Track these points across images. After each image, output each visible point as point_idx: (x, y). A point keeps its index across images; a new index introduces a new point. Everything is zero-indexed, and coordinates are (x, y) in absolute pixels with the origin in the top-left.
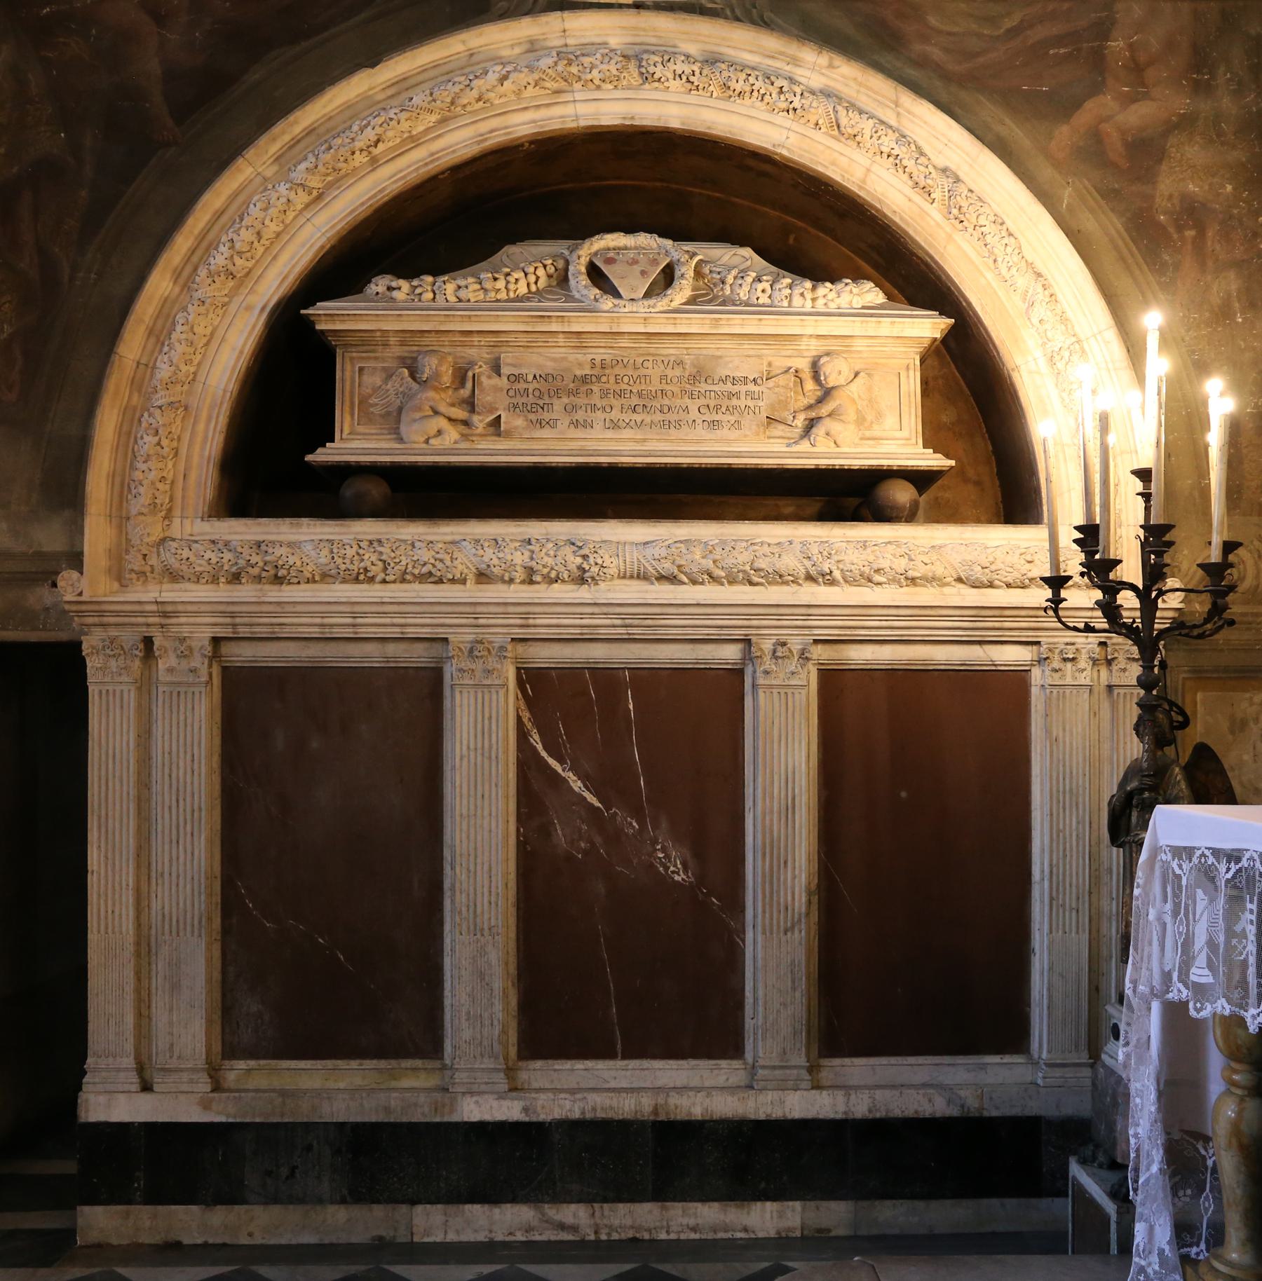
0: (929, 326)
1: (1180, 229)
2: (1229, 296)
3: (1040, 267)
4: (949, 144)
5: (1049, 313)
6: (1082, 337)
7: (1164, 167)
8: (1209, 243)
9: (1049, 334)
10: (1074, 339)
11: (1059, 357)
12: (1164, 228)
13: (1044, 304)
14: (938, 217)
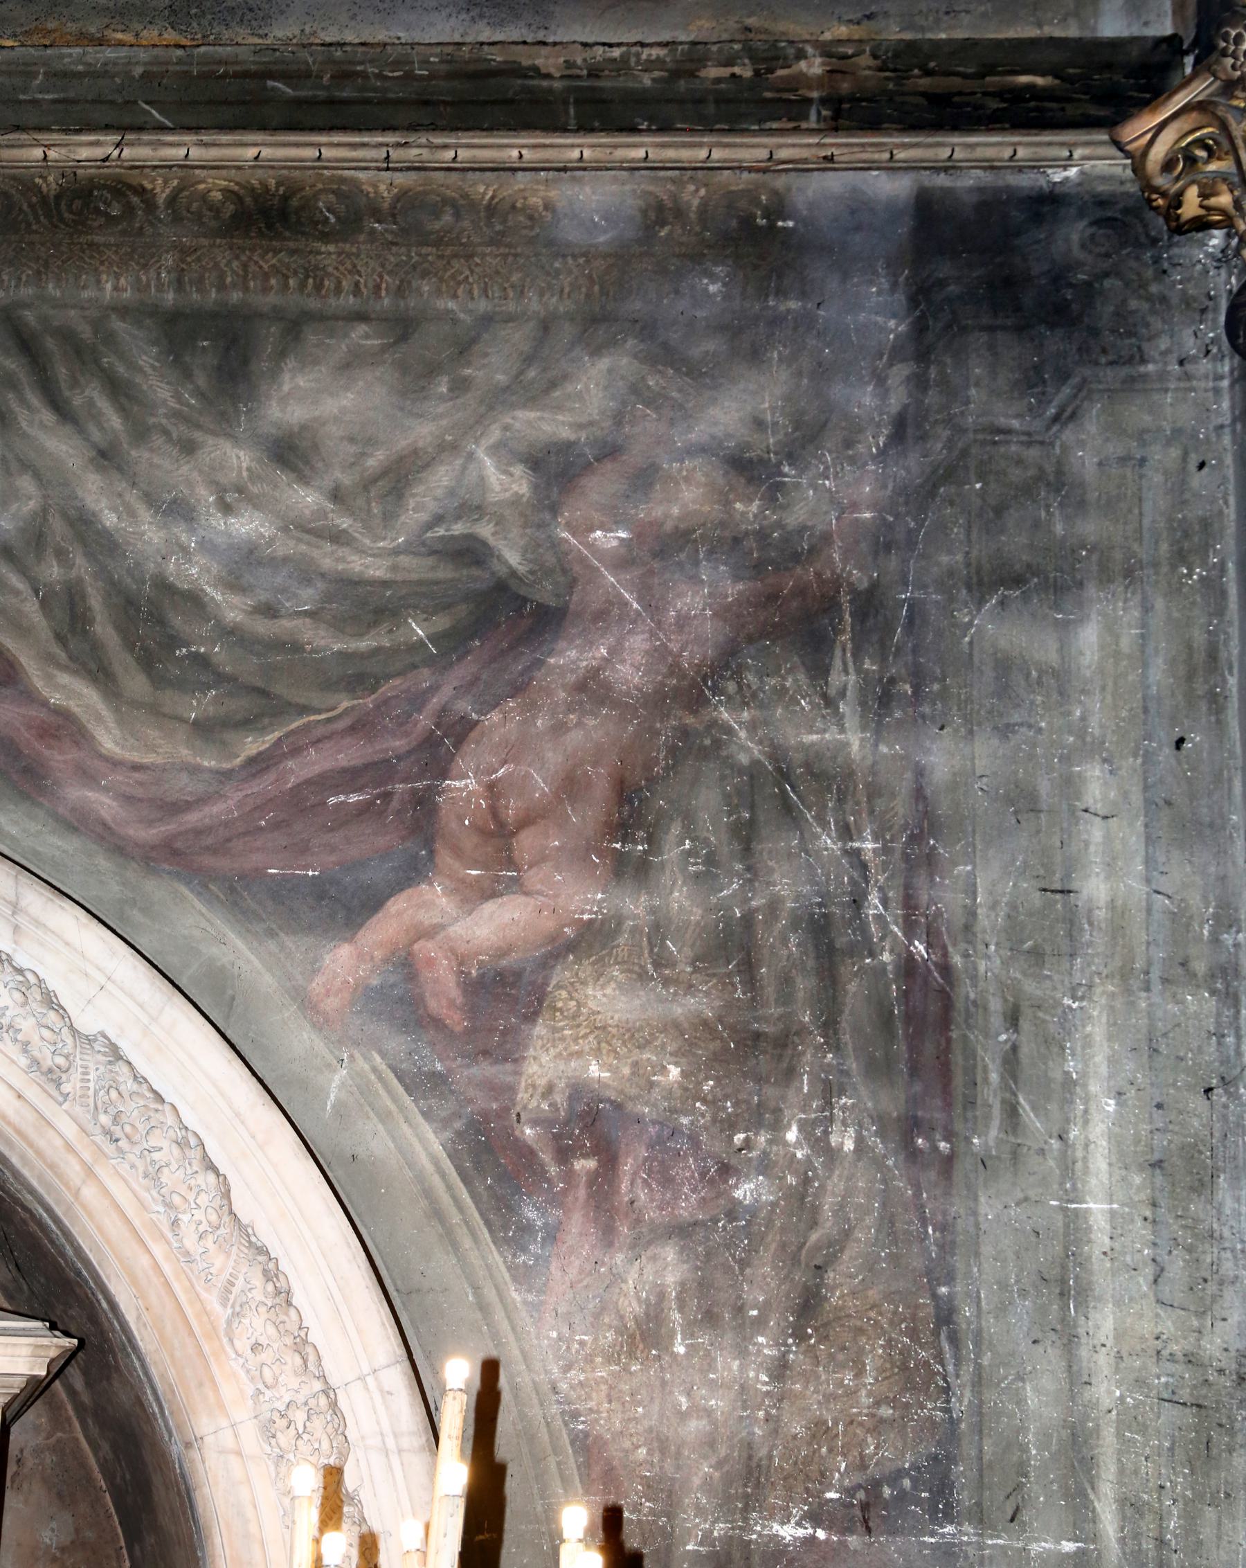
0: (26, 1351)
1: (564, 1155)
2: (662, 1296)
3: (265, 1235)
4: (109, 986)
5: (271, 1330)
6: (334, 1381)
7: (540, 1029)
8: (624, 1186)
9: (267, 1373)
10: (318, 1386)
11: (284, 1422)
12: (532, 1152)
13: (263, 1309)
14: (69, 1130)
